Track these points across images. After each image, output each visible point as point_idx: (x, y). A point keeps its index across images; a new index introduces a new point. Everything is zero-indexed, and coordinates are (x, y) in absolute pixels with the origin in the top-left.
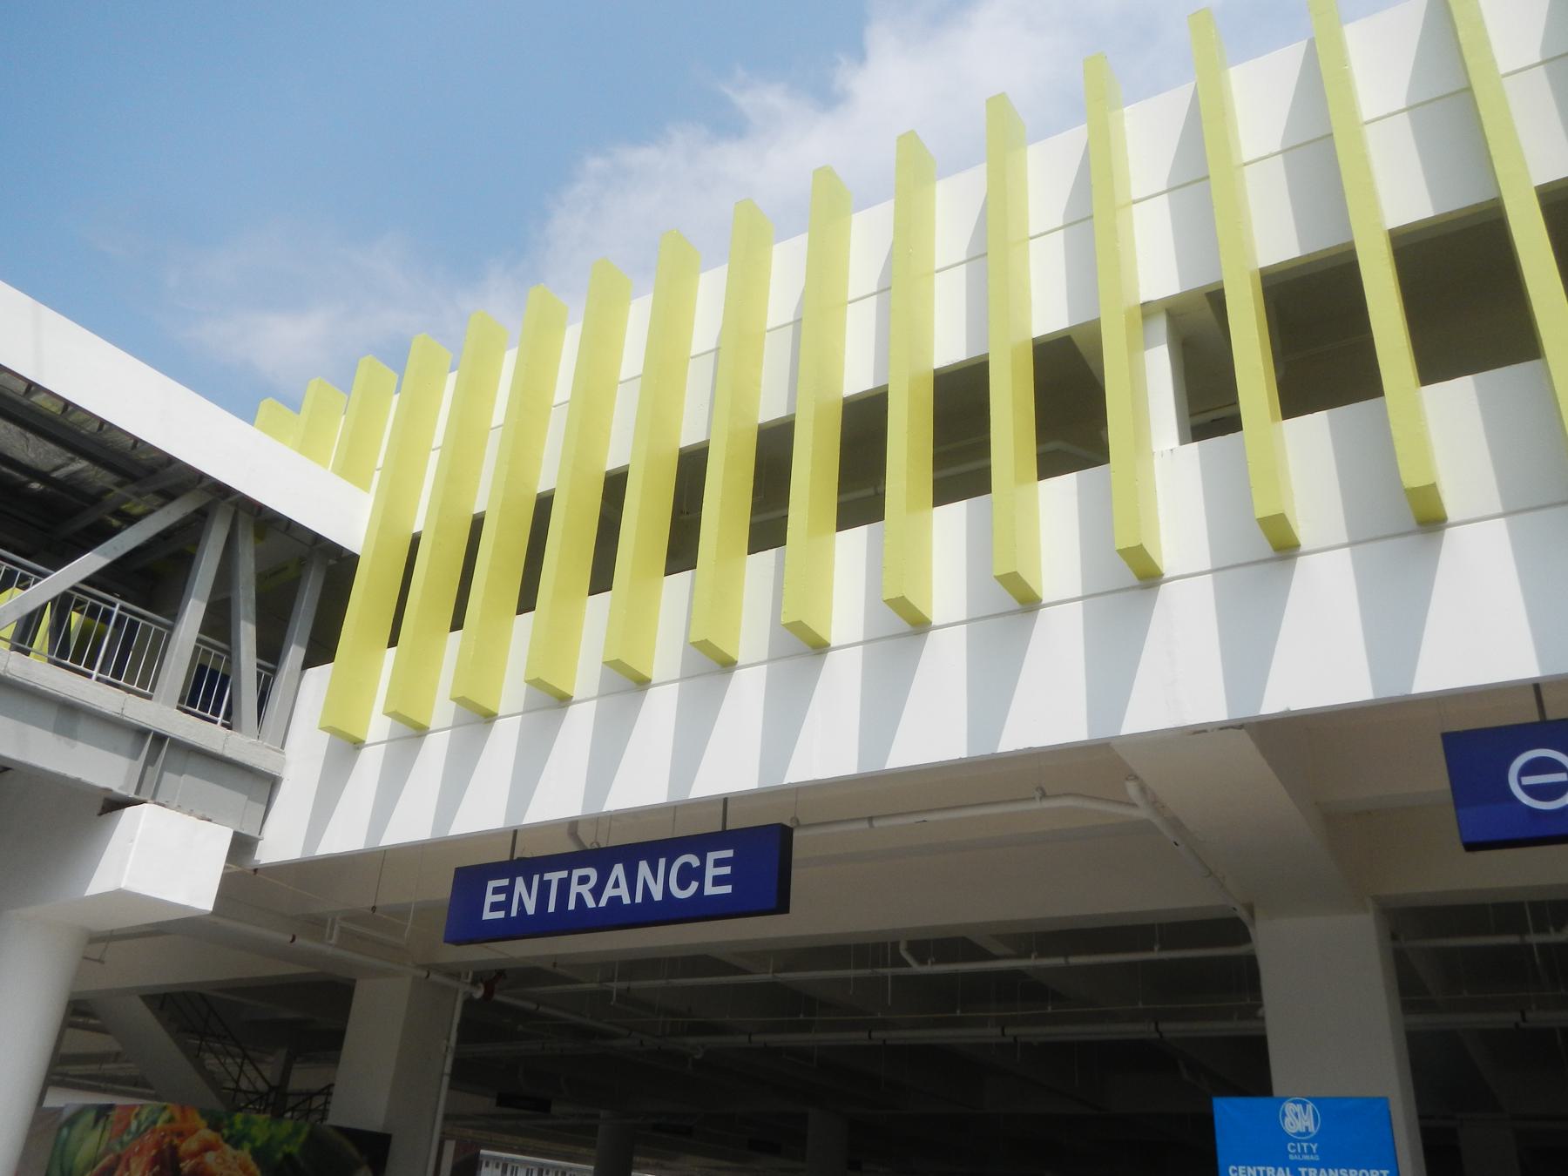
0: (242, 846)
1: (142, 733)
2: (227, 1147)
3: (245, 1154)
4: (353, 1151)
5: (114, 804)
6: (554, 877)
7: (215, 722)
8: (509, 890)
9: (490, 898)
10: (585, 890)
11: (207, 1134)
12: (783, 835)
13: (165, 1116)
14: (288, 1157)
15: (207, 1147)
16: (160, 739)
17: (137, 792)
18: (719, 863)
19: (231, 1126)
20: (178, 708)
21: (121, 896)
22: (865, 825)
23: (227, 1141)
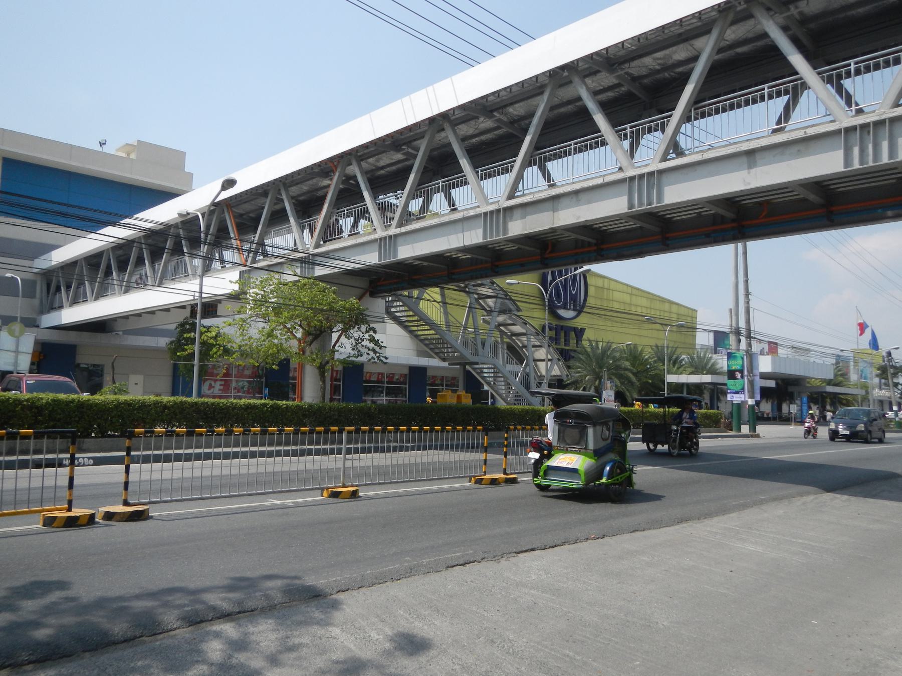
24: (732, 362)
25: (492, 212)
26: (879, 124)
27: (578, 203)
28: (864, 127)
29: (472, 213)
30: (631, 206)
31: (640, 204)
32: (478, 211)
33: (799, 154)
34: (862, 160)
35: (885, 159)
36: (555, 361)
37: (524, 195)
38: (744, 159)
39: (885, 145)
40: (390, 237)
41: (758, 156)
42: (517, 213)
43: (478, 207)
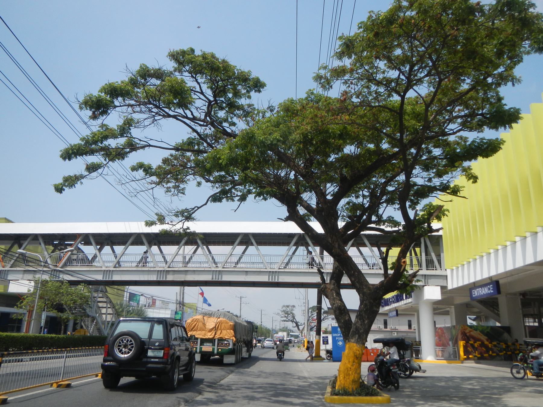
0: (443, 288)
1: (423, 275)
2: (474, 331)
3: (478, 332)
4: (502, 330)
5: (424, 286)
6: (478, 289)
7: (433, 270)
8: (474, 292)
9: (473, 293)
10: (480, 292)
11: (469, 329)
12: (497, 282)
13: (461, 327)
14: (487, 332)
15: (470, 331)
16: (425, 275)
17: (425, 283)
18: (492, 287)
19: (474, 327)
20: (427, 270)
21: (427, 300)
22: (517, 275)
23: (474, 330)
24: (176, 316)
25: (161, 271)
26: (276, 272)
27: (194, 274)
28: (273, 272)
29: (152, 269)
30: (213, 279)
31: (216, 278)
32: (155, 269)
33: (258, 275)
34: (272, 280)
35: (276, 281)
36: (114, 314)
37: (173, 267)
38: (245, 273)
39: (277, 277)
40: (110, 271)
41: (248, 272)
42: (171, 273)
43: (155, 267)
